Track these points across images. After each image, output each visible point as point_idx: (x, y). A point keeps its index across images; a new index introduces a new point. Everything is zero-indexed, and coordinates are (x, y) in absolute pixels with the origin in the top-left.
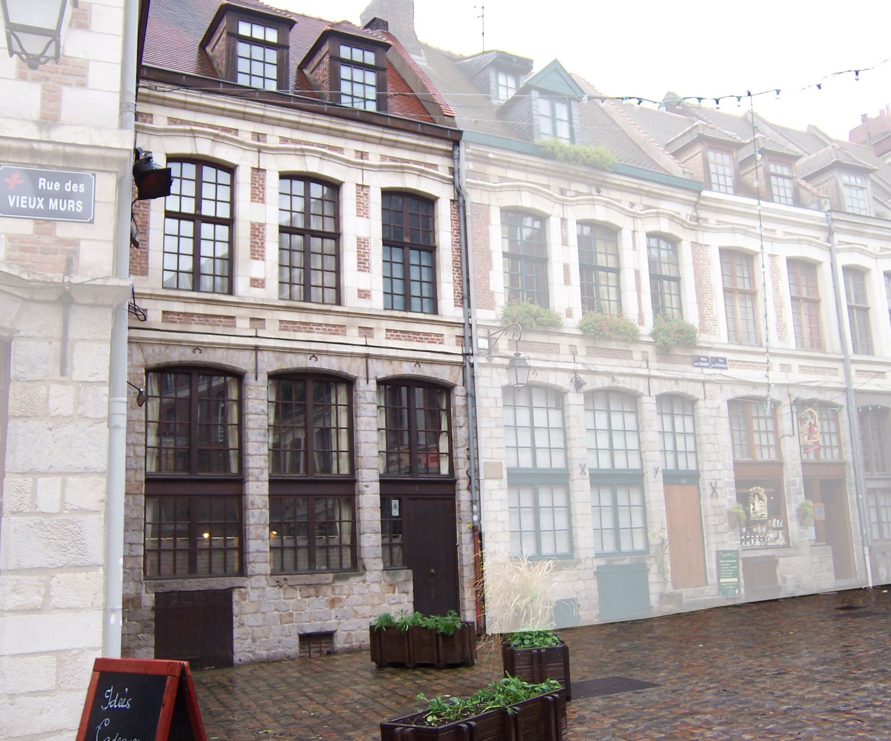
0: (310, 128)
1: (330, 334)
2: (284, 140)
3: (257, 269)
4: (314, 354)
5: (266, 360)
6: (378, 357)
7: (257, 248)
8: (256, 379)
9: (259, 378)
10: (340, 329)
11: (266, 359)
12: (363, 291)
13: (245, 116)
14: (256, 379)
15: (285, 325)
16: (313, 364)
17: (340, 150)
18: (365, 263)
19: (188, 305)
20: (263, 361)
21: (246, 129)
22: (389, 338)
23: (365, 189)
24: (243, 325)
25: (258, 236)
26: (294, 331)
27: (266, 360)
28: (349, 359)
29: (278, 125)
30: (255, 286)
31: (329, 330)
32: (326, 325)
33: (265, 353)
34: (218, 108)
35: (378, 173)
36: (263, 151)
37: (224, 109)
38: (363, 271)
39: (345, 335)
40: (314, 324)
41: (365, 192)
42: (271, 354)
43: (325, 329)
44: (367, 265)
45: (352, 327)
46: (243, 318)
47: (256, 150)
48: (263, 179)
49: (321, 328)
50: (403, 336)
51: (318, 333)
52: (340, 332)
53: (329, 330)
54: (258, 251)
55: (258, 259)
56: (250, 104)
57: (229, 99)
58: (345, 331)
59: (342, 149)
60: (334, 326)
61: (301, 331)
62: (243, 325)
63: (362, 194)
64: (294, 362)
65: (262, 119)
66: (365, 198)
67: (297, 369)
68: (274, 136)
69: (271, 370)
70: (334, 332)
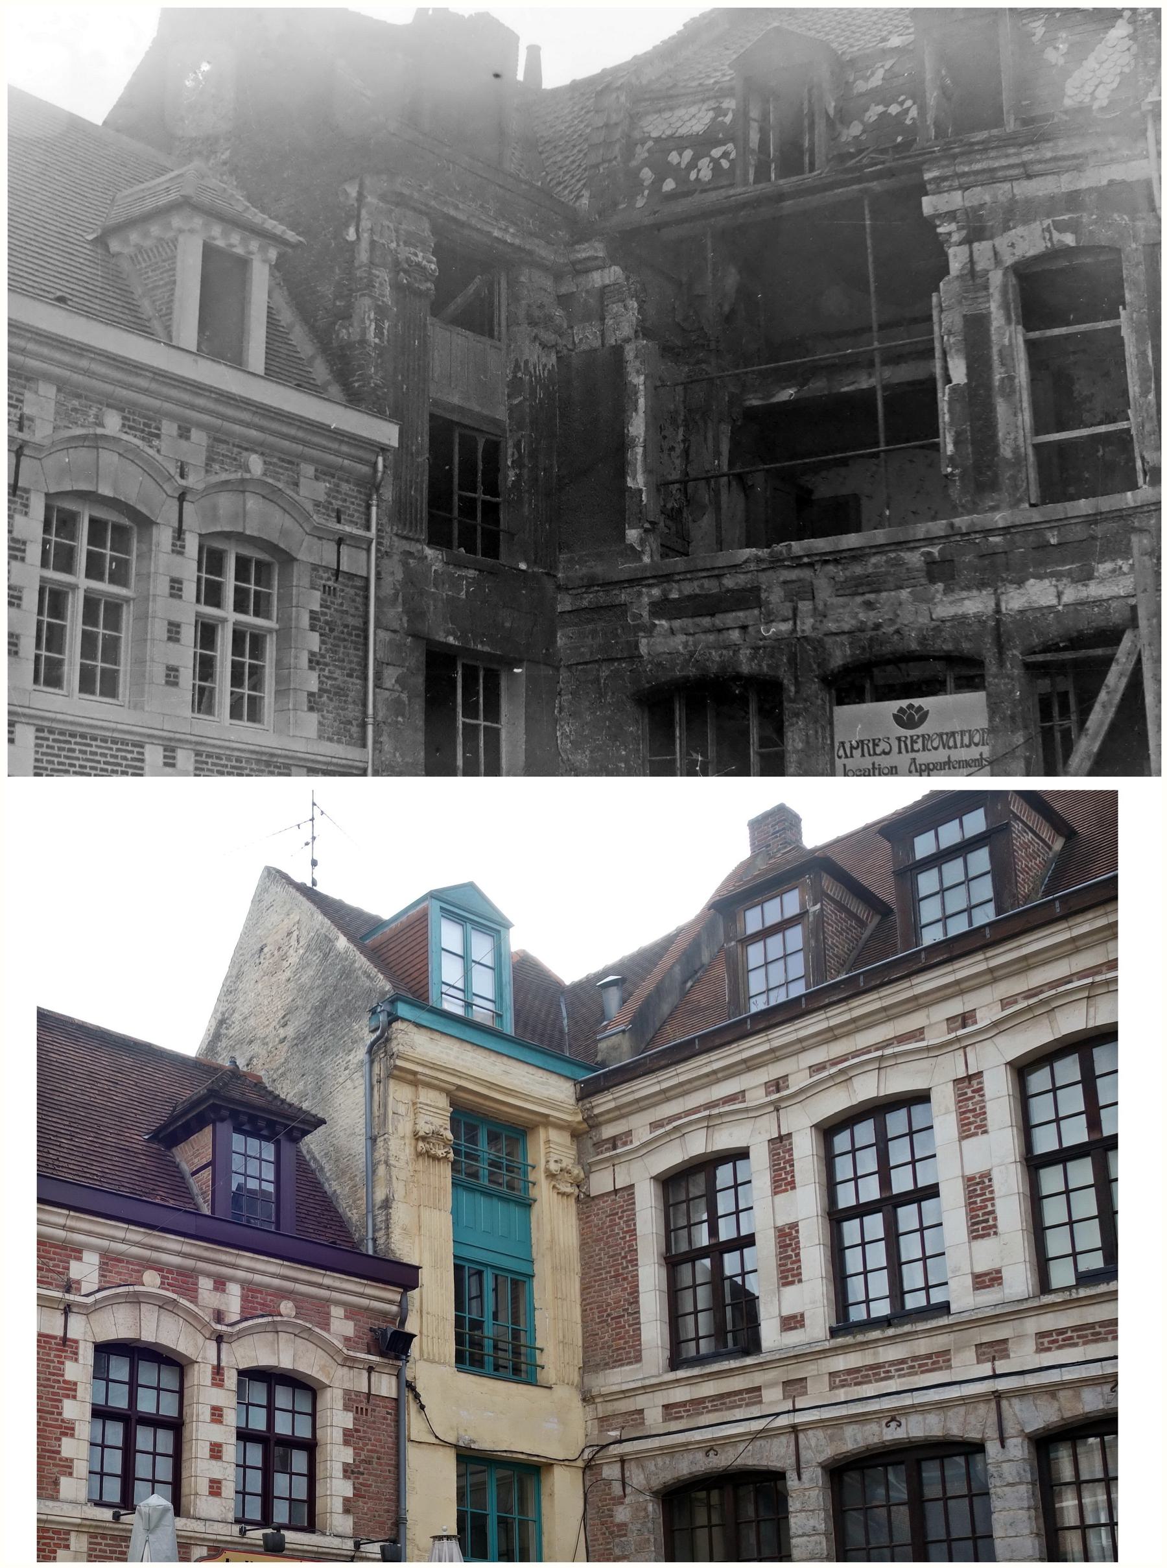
0: (856, 1026)
1: (922, 1372)
2: (815, 1069)
3: (794, 1299)
4: (894, 1417)
5: (813, 1444)
6: (1022, 1393)
7: (789, 1266)
8: (800, 1478)
9: (804, 1477)
10: (940, 1359)
11: (813, 1442)
12: (986, 1274)
13: (749, 1065)
14: (800, 1478)
15: (837, 1379)
16: (893, 1434)
17: (918, 1034)
18: (987, 1221)
19: (693, 1388)
20: (810, 1448)
21: (754, 1082)
22: (1049, 1349)
23: (974, 1082)
24: (773, 1397)
25: (790, 1245)
26: (856, 1384)
27: (813, 1444)
28: (962, 1410)
29: (804, 1050)
30: (791, 1329)
31: (920, 1366)
32: (915, 1358)
33: (810, 1433)
34: (707, 1075)
35: (998, 1040)
36: (783, 1105)
37: (714, 1072)
38: (982, 1236)
39: (949, 1367)
40: (892, 1363)
41: (976, 1087)
42: (820, 1433)
43: (913, 1367)
44: (991, 1223)
45: (959, 1349)
46: (771, 1385)
47: (772, 1109)
48: (790, 1150)
49: (905, 1366)
50: (1079, 1337)
51: (900, 1376)
52: (941, 1364)
53: (920, 1366)
54: (793, 1269)
55: (792, 1283)
56: (745, 1044)
57: (714, 1055)
58: (1006, 1350)
59: (921, 1030)
60: (929, 1356)
61: (870, 1382)
62: (773, 1397)
63: (970, 1094)
64: (859, 1437)
65: (774, 1055)
66: (977, 1098)
67: (868, 1448)
68: (797, 1071)
69: (822, 1458)
70: (930, 1367)
